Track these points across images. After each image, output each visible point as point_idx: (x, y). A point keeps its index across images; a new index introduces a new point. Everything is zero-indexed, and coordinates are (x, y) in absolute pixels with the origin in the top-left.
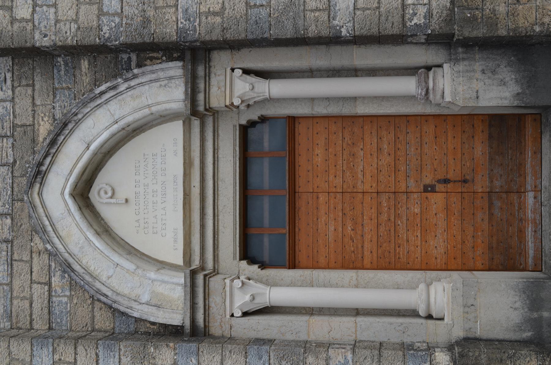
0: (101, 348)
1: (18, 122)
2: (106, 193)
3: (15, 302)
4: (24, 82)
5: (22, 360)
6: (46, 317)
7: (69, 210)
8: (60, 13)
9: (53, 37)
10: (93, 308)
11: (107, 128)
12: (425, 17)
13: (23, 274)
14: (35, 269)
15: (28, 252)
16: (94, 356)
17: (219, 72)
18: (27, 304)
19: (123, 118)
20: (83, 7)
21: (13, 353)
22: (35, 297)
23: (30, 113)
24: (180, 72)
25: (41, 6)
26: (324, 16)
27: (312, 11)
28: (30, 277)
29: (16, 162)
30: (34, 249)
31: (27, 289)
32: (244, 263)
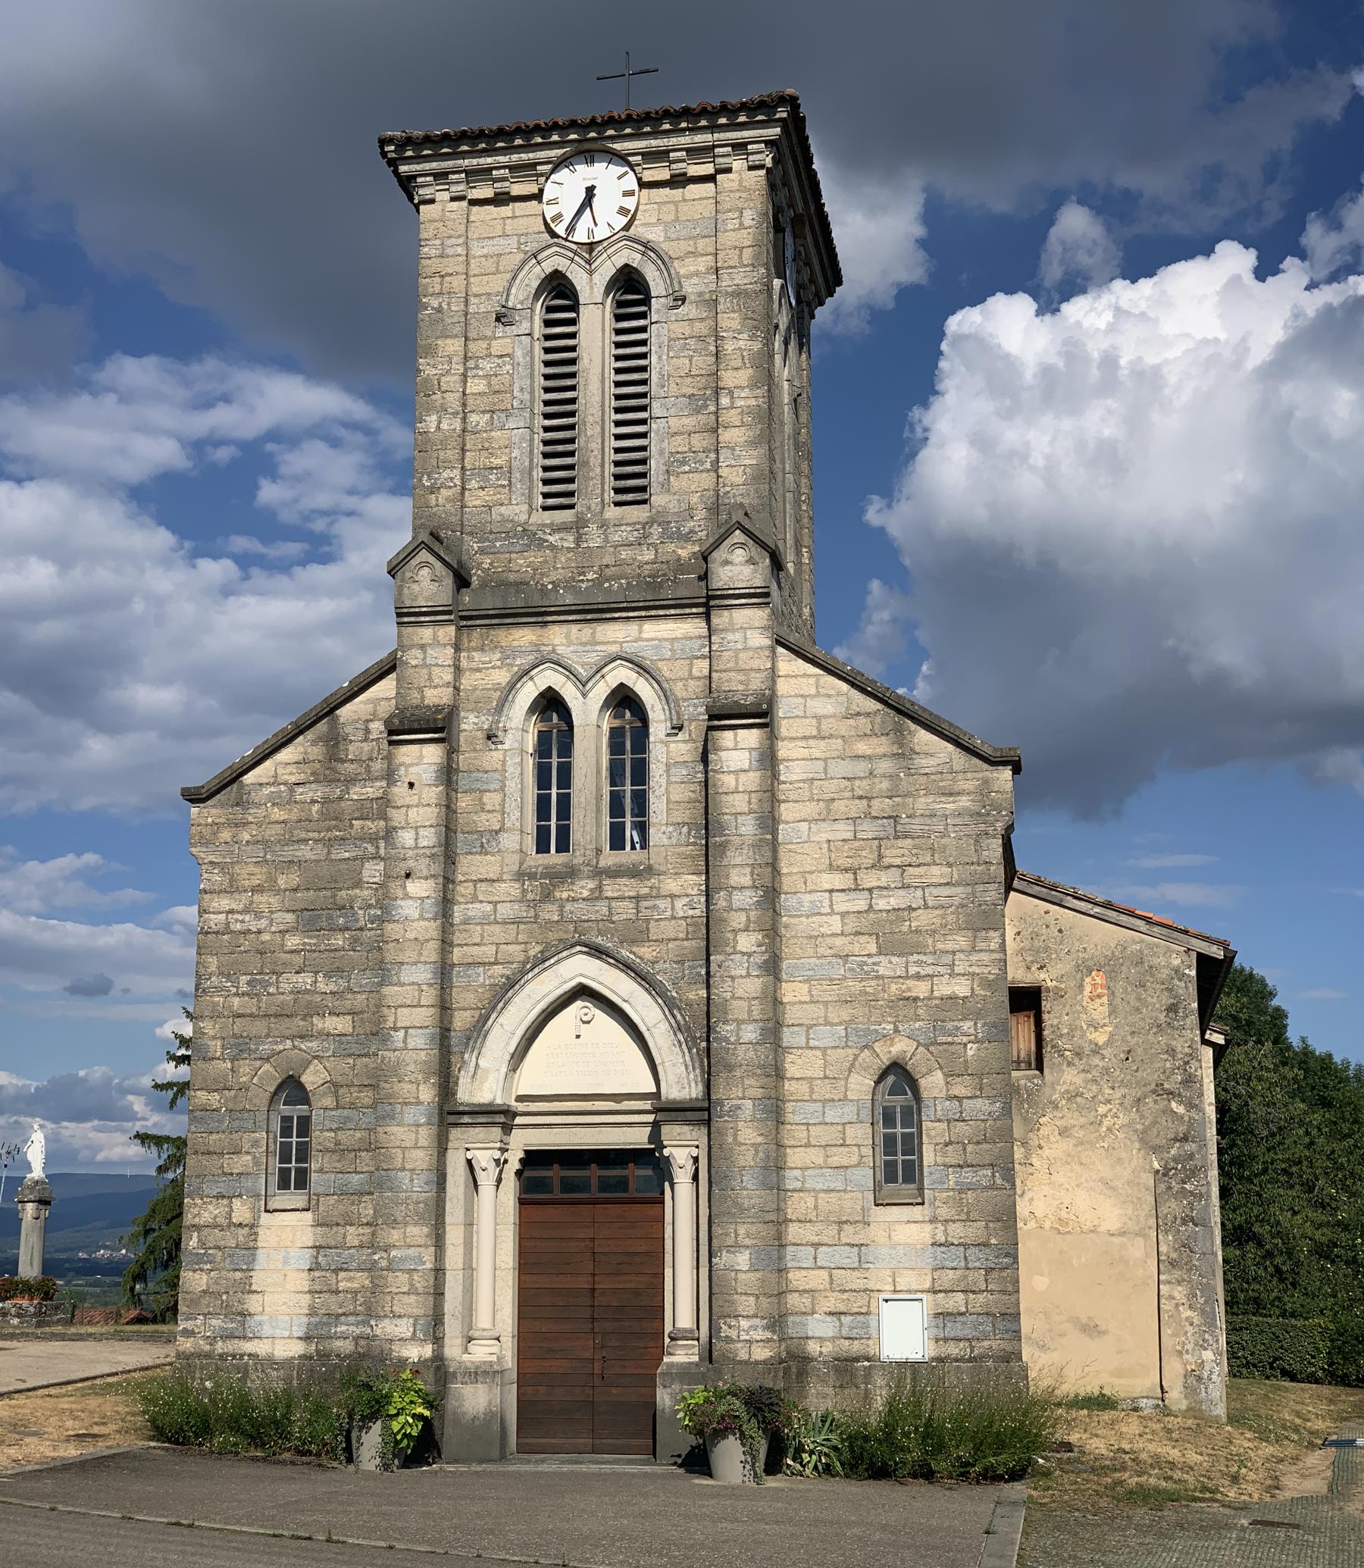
1: (652, 924)
2: (586, 1014)
3: (479, 928)
4: (690, 929)
6: (465, 961)
7: (565, 982)
8: (741, 980)
9: (718, 975)
10: (474, 1009)
11: (643, 1020)
12: (727, 1337)
15: (526, 940)
16: (426, 1024)
17: (694, 1133)
18: (477, 940)
19: (653, 1037)
20: (746, 1004)
22: (483, 948)
24: (694, 1096)
25: (748, 962)
26: (730, 1241)
27: (736, 1230)
30: (528, 946)
32: (521, 1155)
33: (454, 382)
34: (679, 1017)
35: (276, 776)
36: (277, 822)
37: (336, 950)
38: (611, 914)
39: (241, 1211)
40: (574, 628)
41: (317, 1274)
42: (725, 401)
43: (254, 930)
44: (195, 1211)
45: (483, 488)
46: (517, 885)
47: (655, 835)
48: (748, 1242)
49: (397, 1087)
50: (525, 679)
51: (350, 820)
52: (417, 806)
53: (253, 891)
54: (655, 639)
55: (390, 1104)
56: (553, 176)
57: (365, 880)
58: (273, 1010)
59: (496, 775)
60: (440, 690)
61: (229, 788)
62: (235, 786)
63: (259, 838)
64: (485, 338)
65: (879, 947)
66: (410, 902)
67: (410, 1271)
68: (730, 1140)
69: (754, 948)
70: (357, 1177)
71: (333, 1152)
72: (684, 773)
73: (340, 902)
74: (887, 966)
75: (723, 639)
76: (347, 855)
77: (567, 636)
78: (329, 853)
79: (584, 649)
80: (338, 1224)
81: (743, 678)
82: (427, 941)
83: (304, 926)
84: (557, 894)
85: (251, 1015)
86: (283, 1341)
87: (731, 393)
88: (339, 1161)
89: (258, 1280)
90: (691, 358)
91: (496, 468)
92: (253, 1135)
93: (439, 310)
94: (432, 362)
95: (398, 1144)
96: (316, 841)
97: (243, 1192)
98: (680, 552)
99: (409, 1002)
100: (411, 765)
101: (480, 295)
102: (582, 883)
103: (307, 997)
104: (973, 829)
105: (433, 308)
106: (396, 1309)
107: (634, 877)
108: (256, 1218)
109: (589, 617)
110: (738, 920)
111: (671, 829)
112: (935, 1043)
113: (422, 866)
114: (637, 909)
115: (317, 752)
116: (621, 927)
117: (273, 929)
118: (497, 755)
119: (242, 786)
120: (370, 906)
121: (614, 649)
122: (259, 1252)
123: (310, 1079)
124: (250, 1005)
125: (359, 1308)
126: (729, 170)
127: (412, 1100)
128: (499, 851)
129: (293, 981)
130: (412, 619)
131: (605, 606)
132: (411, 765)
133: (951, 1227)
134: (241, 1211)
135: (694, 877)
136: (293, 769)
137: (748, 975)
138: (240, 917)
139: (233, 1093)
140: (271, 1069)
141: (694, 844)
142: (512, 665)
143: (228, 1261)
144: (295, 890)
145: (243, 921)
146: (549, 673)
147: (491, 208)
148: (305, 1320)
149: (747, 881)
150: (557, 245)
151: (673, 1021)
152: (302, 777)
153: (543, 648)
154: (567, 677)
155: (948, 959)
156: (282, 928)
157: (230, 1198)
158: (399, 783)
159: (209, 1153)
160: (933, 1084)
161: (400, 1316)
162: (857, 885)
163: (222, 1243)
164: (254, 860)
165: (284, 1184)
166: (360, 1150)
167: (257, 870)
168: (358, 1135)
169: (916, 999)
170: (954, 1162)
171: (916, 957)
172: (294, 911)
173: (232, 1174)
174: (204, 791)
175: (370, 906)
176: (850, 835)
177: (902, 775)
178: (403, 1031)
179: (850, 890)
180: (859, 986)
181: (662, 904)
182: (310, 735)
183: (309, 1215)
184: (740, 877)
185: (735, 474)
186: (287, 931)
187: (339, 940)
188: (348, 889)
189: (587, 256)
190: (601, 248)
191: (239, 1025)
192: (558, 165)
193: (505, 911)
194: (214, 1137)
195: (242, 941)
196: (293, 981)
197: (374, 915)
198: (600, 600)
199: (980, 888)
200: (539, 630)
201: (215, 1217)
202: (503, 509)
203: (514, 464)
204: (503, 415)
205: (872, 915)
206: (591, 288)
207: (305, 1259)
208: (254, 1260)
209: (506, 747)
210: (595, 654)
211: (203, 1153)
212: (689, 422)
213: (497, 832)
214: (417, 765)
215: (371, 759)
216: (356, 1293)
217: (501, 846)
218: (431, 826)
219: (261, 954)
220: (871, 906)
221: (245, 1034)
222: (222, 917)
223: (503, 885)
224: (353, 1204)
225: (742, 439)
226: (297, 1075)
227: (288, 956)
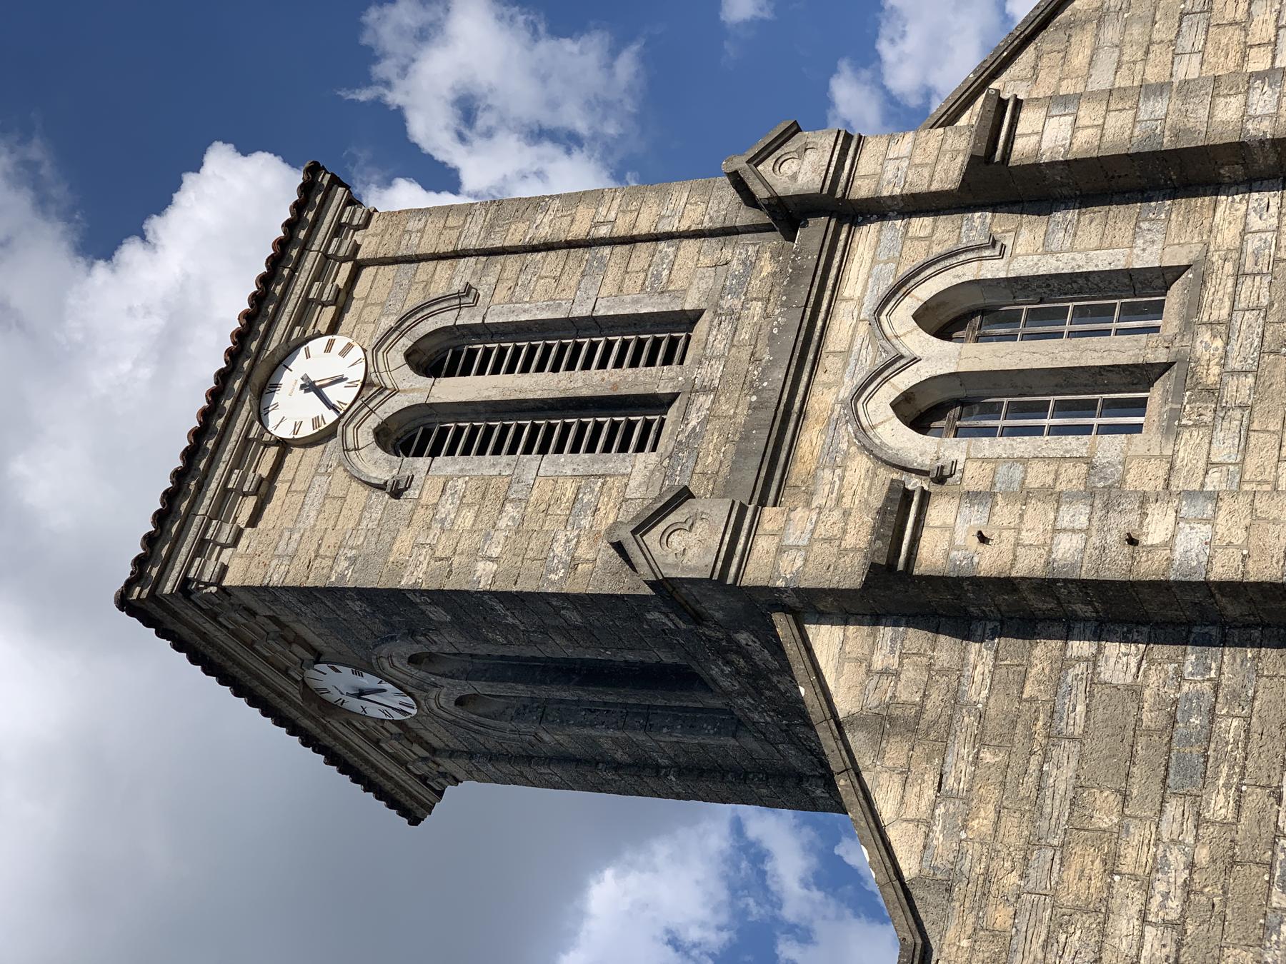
5: (1275, 519)
13: (1266, 450)
21: (1258, 511)
28: (1277, 454)
29: (1273, 304)
31: (1270, 469)
33: (448, 540)
35: (918, 822)
36: (997, 824)
37: (1247, 731)
38: (1258, 308)
40: (821, 377)
42: (603, 231)
43: (1185, 874)
45: (597, 509)
46: (1186, 435)
47: (1147, 256)
50: (871, 434)
51: (1020, 700)
52: (1019, 531)
53: (1112, 873)
54: (867, 282)
56: (269, 429)
57: (1129, 680)
59: (1003, 469)
60: (851, 524)
61: (918, 904)
62: (916, 893)
63: (1019, 856)
64: (413, 511)
66: (1180, 539)
72: (1061, 235)
73: (1163, 721)
75: (889, 183)
76: (1080, 708)
77: (828, 386)
78: (1072, 738)
79: (851, 367)
81: (948, 156)
82: (1253, 510)
83: (1194, 784)
84: (1212, 379)
87: (597, 225)
90: (541, 277)
91: (577, 494)
93: (353, 561)
94: (410, 569)
96: (1046, 758)
98: (764, 274)
100: (951, 541)
101: (360, 520)
102: (1199, 348)
105: (347, 568)
107: (1204, 282)
109: (811, 357)
111: (1140, 242)
113: (1122, 522)
114: (1255, 275)
115: (895, 751)
118: (972, 469)
119: (920, 878)
120: (1179, 674)
121: (863, 328)
126: (357, 248)
128: (1123, 463)
130: (736, 561)
131: (803, 333)
132: (951, 541)
136: (912, 791)
138: (1157, 899)
141: (1170, 212)
142: (847, 454)
144: (1125, 798)
145: (1166, 896)
147: (269, 507)
149: (1236, 102)
150: (346, 425)
152: (931, 779)
153: (835, 415)
154: (885, 380)
156: (1190, 824)
158: (976, 560)
162: (1269, 43)
164: (1056, 867)
167: (1076, 864)
172: (1163, 801)
174: (910, 939)
175: (1179, 674)
176: (1196, 59)
177: (1126, 15)
179: (1274, 51)
181: (1253, 243)
182: (864, 761)
185: (691, 214)
186: (1199, 814)
187: (1231, 727)
188: (1140, 708)
189: (375, 389)
190: (373, 376)
192: (260, 415)
193: (1225, 449)
195: (1203, 899)
197: (1195, 665)
198: (793, 338)
202: (632, 484)
203: (581, 471)
204: (515, 487)
206: (413, 390)
210: (864, 352)
212: (613, 272)
213: (1091, 466)
214: (953, 532)
218: (1057, 510)
219: (1233, 863)
223: (1181, 454)
225: (655, 208)
227: (1245, 814)
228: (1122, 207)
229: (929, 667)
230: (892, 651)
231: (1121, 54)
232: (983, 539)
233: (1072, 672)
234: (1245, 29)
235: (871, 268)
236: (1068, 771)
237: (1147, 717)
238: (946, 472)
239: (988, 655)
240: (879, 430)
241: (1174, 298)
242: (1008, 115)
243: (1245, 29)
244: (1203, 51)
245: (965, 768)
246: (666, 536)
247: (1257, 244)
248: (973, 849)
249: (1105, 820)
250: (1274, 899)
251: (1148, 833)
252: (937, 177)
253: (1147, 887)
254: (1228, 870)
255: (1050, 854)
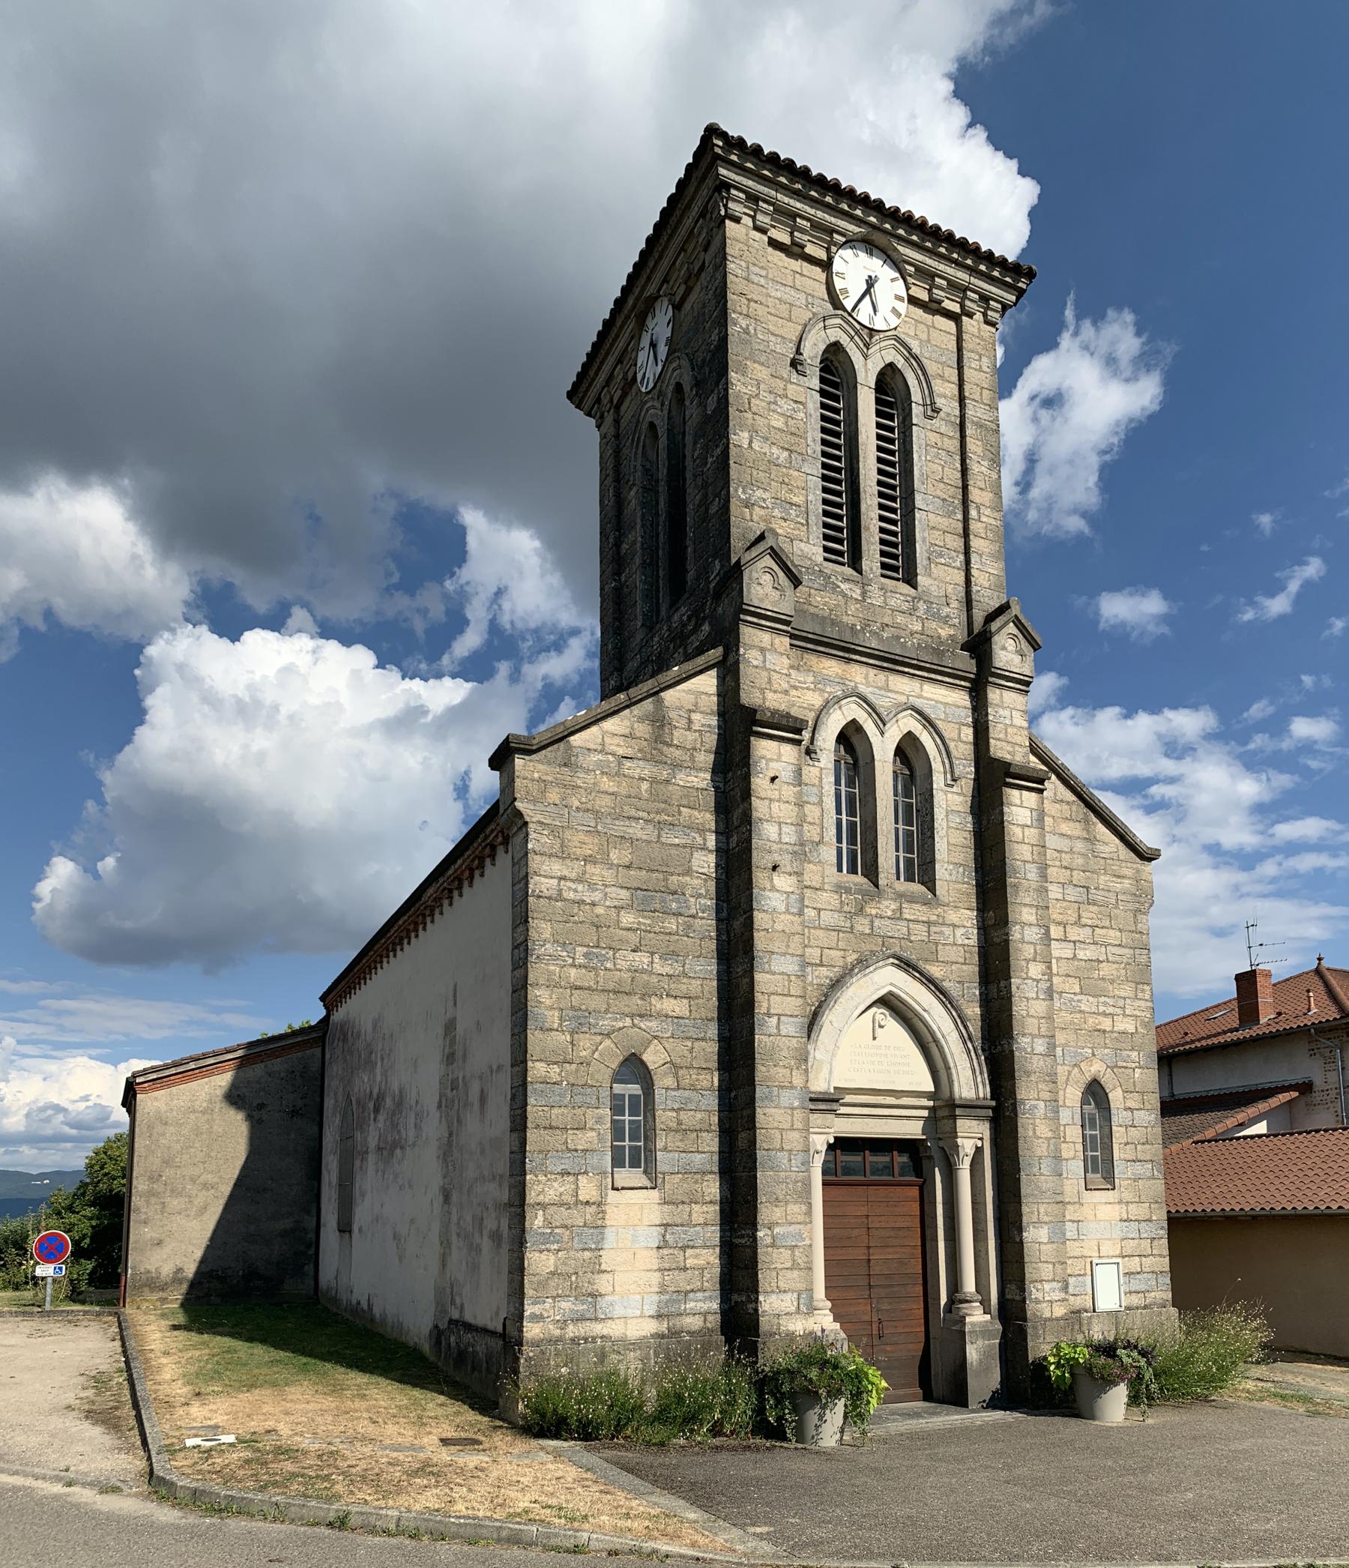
0: (801, 1020)
1: (940, 947)
14: (832, 952)
23: (947, 959)
34: (971, 1029)
37: (670, 933)
39: (588, 1189)
40: (872, 672)
41: (665, 1251)
43: (588, 901)
44: (539, 1188)
46: (836, 897)
47: (942, 871)
48: (1046, 1219)
49: (773, 1071)
50: (836, 706)
52: (778, 801)
53: (585, 860)
55: (768, 1087)
58: (611, 986)
59: (815, 790)
60: (780, 695)
63: (589, 807)
65: (1081, 988)
66: (777, 895)
67: (793, 1248)
68: (1031, 1133)
69: (1040, 977)
70: (699, 1156)
71: (676, 1131)
73: (673, 888)
74: (1087, 1004)
76: (677, 841)
77: (866, 677)
78: (659, 836)
79: (878, 692)
80: (683, 1203)
82: (794, 934)
83: (638, 905)
84: (868, 910)
85: (589, 989)
86: (635, 1321)
88: (681, 1140)
89: (608, 1259)
92: (597, 1111)
95: (776, 1125)
97: (589, 1169)
98: (940, 631)
99: (780, 991)
102: (886, 903)
103: (645, 977)
104: (1130, 906)
106: (781, 1284)
107: (925, 904)
108: (603, 1196)
109: (885, 665)
110: (1028, 951)
111: (951, 867)
112: (1116, 1066)
115: (643, 730)
116: (915, 945)
117: (608, 903)
118: (815, 771)
120: (700, 896)
121: (903, 699)
122: (606, 1231)
123: (653, 1057)
124: (587, 979)
125: (706, 1284)
127: (786, 1084)
128: (820, 862)
129: (628, 959)
131: (901, 659)
133: (1131, 1206)
134: (588, 1189)
135: (968, 912)
137: (1038, 998)
138: (574, 886)
139: (574, 1066)
140: (612, 1045)
141: (968, 883)
142: (824, 691)
143: (576, 1240)
146: (854, 706)
148: (656, 1298)
149: (1032, 919)
151: (964, 1031)
152: (629, 752)
153: (847, 682)
154: (870, 715)
155: (1121, 1003)
156: (616, 903)
157: (576, 1175)
159: (551, 1127)
160: (1116, 1097)
161: (785, 1292)
163: (569, 1222)
164: (585, 828)
165: (617, 1162)
166: (701, 1130)
168: (699, 1116)
169: (1104, 1031)
170: (1130, 1158)
171: (1102, 999)
173: (576, 1150)
175: (700, 896)
176: (1060, 896)
178: (776, 1018)
180: (1069, 1017)
181: (947, 931)
182: (636, 710)
183: (655, 1194)
184: (1028, 915)
187: (672, 925)
188: (679, 875)
191: (577, 998)
193: (827, 918)
194: (555, 1111)
195: (576, 911)
196: (628, 959)
198: (898, 652)
199: (1138, 951)
200: (844, 666)
201: (561, 1194)
205: (1076, 963)
207: (653, 1237)
208: (603, 1239)
209: (821, 765)
211: (545, 1128)
213: (818, 844)
215: (695, 749)
216: (703, 1269)
217: (821, 857)
218: (792, 824)
220: (1075, 956)
221: (583, 1007)
222: (555, 882)
224: (696, 1182)
226: (638, 1053)
228: (972, 856)
229: (695, 749)
230: (703, 725)
231: (1066, 853)
232: (773, 779)
233: (697, 836)
234: (1075, 923)
235: (941, 703)
236: (640, 834)
237: (674, 878)
238: (813, 756)
239: (703, 784)
240: (839, 712)
241: (917, 888)
242: (1035, 785)
243: (1075, 923)
244: (1064, 900)
245: (637, 773)
246: (769, 571)
247: (947, 933)
248: (590, 778)
249: (614, 856)
250: (580, 949)
251: (610, 880)
252: (998, 743)
253: (579, 880)
254: (593, 924)
255: (592, 824)
